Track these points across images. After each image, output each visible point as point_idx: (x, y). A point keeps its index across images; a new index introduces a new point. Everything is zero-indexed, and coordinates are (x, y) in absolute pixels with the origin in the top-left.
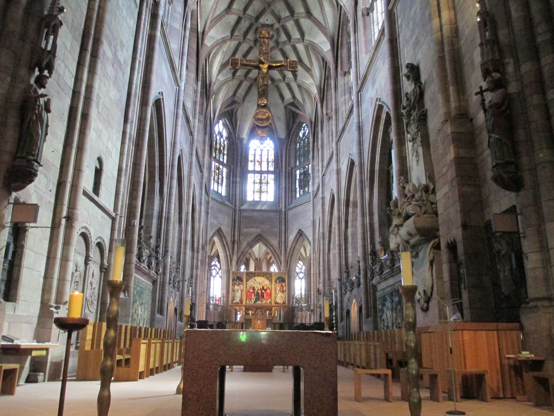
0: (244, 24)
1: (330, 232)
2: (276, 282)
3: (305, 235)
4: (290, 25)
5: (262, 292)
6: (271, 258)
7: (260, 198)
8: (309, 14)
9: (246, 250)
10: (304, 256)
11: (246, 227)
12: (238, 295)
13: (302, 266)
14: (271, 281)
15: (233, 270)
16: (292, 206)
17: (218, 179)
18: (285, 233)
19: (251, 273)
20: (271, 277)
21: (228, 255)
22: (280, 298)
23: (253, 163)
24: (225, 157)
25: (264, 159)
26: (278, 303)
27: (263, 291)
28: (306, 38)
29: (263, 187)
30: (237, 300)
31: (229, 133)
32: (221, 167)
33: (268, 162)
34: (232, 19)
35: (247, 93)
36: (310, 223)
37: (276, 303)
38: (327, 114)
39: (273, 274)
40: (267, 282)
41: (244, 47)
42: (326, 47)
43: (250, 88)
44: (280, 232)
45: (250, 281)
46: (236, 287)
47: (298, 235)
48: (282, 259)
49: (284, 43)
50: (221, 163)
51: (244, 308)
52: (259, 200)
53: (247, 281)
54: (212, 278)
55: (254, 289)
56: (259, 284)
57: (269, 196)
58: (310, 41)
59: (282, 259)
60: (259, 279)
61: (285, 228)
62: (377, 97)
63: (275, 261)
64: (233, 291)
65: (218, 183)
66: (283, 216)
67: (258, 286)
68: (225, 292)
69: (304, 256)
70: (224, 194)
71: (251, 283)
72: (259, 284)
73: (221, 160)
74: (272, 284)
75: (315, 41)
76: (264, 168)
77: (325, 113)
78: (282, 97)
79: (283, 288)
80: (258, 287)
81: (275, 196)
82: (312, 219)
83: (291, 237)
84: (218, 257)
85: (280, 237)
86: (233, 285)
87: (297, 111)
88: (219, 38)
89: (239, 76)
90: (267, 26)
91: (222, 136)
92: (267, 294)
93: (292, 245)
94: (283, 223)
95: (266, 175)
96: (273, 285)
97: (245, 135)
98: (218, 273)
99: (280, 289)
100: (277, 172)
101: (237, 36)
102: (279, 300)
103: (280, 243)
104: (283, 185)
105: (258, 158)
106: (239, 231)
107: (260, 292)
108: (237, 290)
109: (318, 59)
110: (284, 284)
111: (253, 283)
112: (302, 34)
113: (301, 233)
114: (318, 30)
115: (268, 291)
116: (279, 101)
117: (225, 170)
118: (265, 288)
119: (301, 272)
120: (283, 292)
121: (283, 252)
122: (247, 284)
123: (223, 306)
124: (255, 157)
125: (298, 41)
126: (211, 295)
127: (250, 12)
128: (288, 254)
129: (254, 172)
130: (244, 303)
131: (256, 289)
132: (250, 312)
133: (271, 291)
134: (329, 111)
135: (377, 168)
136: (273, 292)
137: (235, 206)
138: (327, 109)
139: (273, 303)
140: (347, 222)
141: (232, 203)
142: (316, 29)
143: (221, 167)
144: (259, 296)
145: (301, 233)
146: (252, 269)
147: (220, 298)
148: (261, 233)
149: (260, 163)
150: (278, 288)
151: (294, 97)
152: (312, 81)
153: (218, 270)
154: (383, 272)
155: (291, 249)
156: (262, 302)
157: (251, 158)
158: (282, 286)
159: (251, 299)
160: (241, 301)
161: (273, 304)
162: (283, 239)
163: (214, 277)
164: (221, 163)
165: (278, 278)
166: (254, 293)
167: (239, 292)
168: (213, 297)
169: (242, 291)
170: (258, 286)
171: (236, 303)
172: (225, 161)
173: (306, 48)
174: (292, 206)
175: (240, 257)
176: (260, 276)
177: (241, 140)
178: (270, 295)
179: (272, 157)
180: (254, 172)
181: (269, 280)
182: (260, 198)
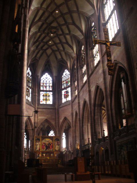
0: (45, 26)
1: (83, 118)
2: (55, 141)
3: (68, 119)
4: (64, 28)
5: (49, 146)
7: (46, 103)
8: (74, 24)
9: (40, 126)
11: (40, 116)
14: (53, 140)
16: (61, 106)
17: (28, 94)
18: (58, 119)
20: (53, 138)
23: (42, 87)
24: (31, 84)
25: (48, 85)
28: (72, 33)
29: (47, 98)
30: (38, 149)
31: (32, 73)
32: (29, 88)
33: (49, 86)
34: (40, 23)
35: (41, 55)
36: (70, 114)
37: (55, 150)
38: (80, 66)
40: (51, 141)
41: (43, 35)
42: (81, 37)
43: (42, 53)
44: (56, 119)
46: (37, 143)
47: (64, 119)
49: (61, 35)
50: (29, 87)
51: (41, 153)
52: (45, 103)
53: (42, 140)
55: (45, 144)
56: (48, 141)
57: (50, 102)
58: (73, 34)
61: (58, 116)
62: (115, 59)
64: (36, 145)
65: (28, 96)
66: (57, 111)
67: (47, 142)
70: (30, 101)
71: (44, 141)
73: (29, 85)
74: (53, 142)
75: (76, 34)
76: (48, 89)
77: (79, 65)
78: (56, 58)
81: (53, 102)
82: (71, 112)
83: (61, 121)
85: (56, 121)
87: (63, 64)
88: (34, 31)
89: (39, 48)
90: (54, 27)
91: (29, 75)
93: (61, 124)
94: (57, 114)
95: (49, 92)
96: (54, 142)
97: (39, 74)
100: (54, 91)
101: (41, 31)
102: (57, 149)
103: (55, 123)
104: (57, 97)
105: (45, 85)
106: (37, 117)
107: (48, 145)
108: (38, 145)
109: (75, 42)
112: (69, 31)
113: (65, 119)
114: (78, 30)
115: (52, 145)
116: (55, 60)
117: (30, 90)
118: (50, 143)
120: (58, 145)
121: (57, 127)
122: (42, 142)
123: (31, 152)
124: (43, 84)
125: (67, 34)
127: (47, 21)
128: (59, 128)
129: (43, 91)
130: (41, 150)
132: (44, 154)
133: (53, 144)
134: (81, 64)
135: (114, 89)
136: (54, 145)
137: (35, 106)
138: (80, 64)
139: (54, 150)
140: (94, 113)
141: (34, 105)
142: (76, 29)
143: (29, 88)
144: (48, 147)
145: (65, 119)
148: (48, 119)
149: (46, 87)
150: (56, 143)
151: (62, 58)
152: (72, 51)
154: (121, 135)
155: (61, 126)
157: (42, 84)
158: (58, 142)
162: (57, 122)
164: (29, 87)
165: (56, 139)
167: (38, 146)
169: (40, 145)
170: (47, 142)
172: (31, 86)
173: (71, 37)
174: (61, 106)
175: (38, 129)
177: (38, 76)
179: (51, 85)
180: (43, 91)
182: (46, 103)
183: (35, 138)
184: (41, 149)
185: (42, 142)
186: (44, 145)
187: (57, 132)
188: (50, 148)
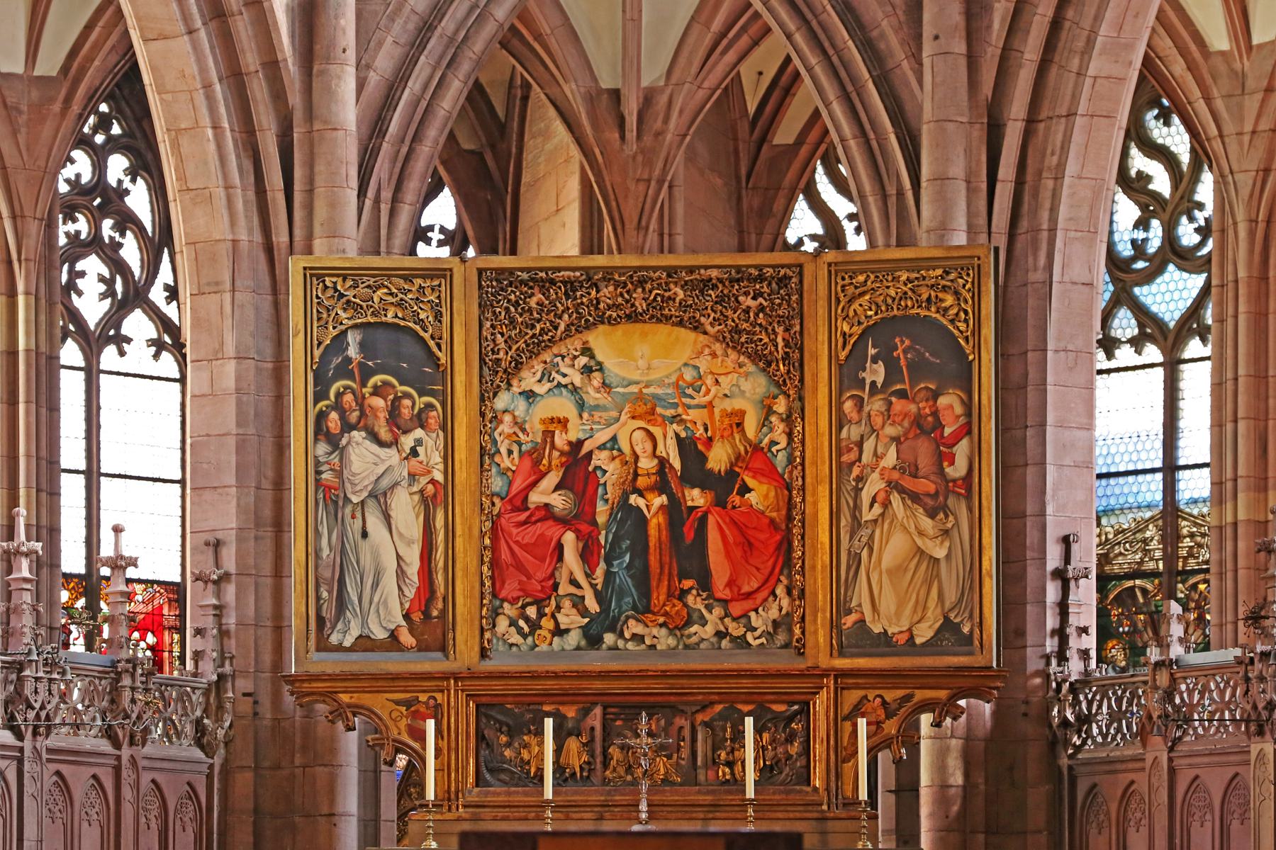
2: (847, 374)
5: (675, 511)
6: (784, 85)
10: (1219, 39)
12: (391, 547)
13: (1184, 181)
15: (322, 255)
19: (543, 279)
21: (251, 60)
22: (899, 574)
26: (884, 642)
27: (696, 497)
30: (385, 610)
39: (817, 283)
45: (529, 379)
46: (365, 459)
48: (938, 90)
53: (496, 373)
54: (71, 353)
55: (577, 470)
56: (646, 409)
59: (938, 90)
60: (643, 357)
63: (838, 118)
67: (630, 434)
68: (226, 518)
69: (1219, 39)
71: (540, 402)
72: (646, 409)
79: (943, 457)
80: (626, 444)
84: (127, 90)
86: (321, 430)
92: (745, 535)
98: (135, 297)
99: (909, 468)
108: (380, 496)
110: (950, 401)
111: (563, 406)
115: (759, 496)
118: (718, 458)
119: (1174, 252)
122: (487, 418)
126: (73, 560)
130: (465, 652)
131: (611, 471)
133: (789, 491)
139: (820, 636)
146: (556, 236)
147: (176, 591)
153: (131, 252)
156: (678, 626)
158: (926, 426)
159: (545, 594)
160: (429, 617)
161: (820, 650)
163: (92, 343)
166: (580, 520)
168: (88, 585)
169: (434, 500)
170: (630, 434)
171: (365, 643)
176: (657, 314)
178: (775, 546)
181: (764, 361)
183: (316, 312)
184: (465, 606)
185: (487, 418)
186: (546, 494)
187: (949, 153)
188: (705, 583)
